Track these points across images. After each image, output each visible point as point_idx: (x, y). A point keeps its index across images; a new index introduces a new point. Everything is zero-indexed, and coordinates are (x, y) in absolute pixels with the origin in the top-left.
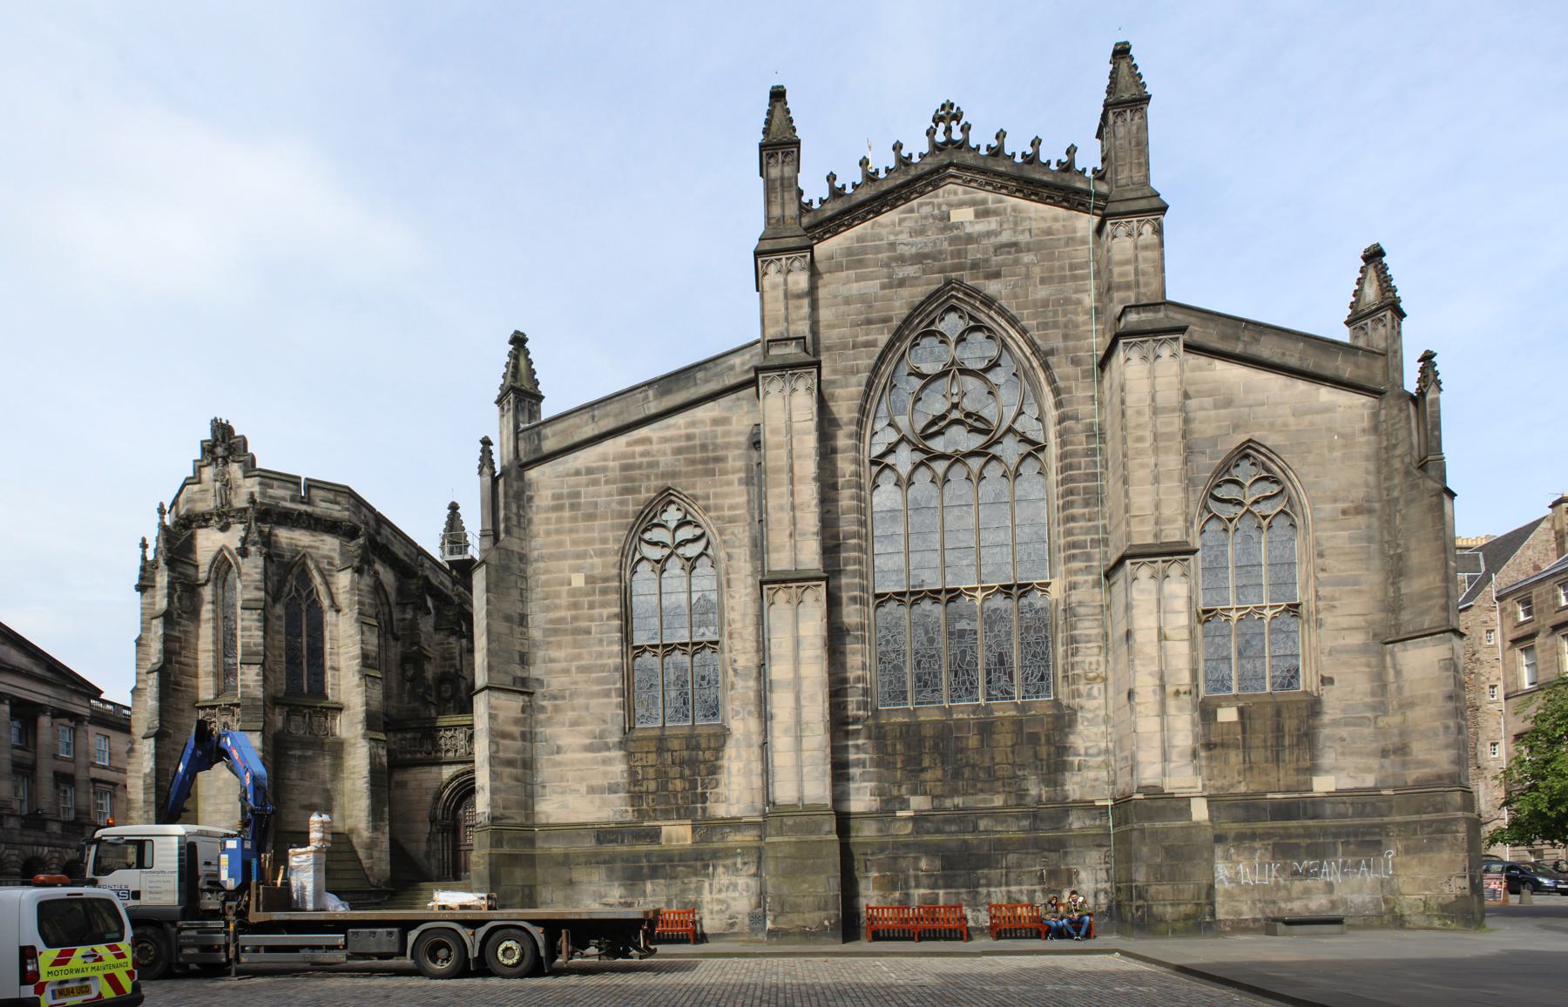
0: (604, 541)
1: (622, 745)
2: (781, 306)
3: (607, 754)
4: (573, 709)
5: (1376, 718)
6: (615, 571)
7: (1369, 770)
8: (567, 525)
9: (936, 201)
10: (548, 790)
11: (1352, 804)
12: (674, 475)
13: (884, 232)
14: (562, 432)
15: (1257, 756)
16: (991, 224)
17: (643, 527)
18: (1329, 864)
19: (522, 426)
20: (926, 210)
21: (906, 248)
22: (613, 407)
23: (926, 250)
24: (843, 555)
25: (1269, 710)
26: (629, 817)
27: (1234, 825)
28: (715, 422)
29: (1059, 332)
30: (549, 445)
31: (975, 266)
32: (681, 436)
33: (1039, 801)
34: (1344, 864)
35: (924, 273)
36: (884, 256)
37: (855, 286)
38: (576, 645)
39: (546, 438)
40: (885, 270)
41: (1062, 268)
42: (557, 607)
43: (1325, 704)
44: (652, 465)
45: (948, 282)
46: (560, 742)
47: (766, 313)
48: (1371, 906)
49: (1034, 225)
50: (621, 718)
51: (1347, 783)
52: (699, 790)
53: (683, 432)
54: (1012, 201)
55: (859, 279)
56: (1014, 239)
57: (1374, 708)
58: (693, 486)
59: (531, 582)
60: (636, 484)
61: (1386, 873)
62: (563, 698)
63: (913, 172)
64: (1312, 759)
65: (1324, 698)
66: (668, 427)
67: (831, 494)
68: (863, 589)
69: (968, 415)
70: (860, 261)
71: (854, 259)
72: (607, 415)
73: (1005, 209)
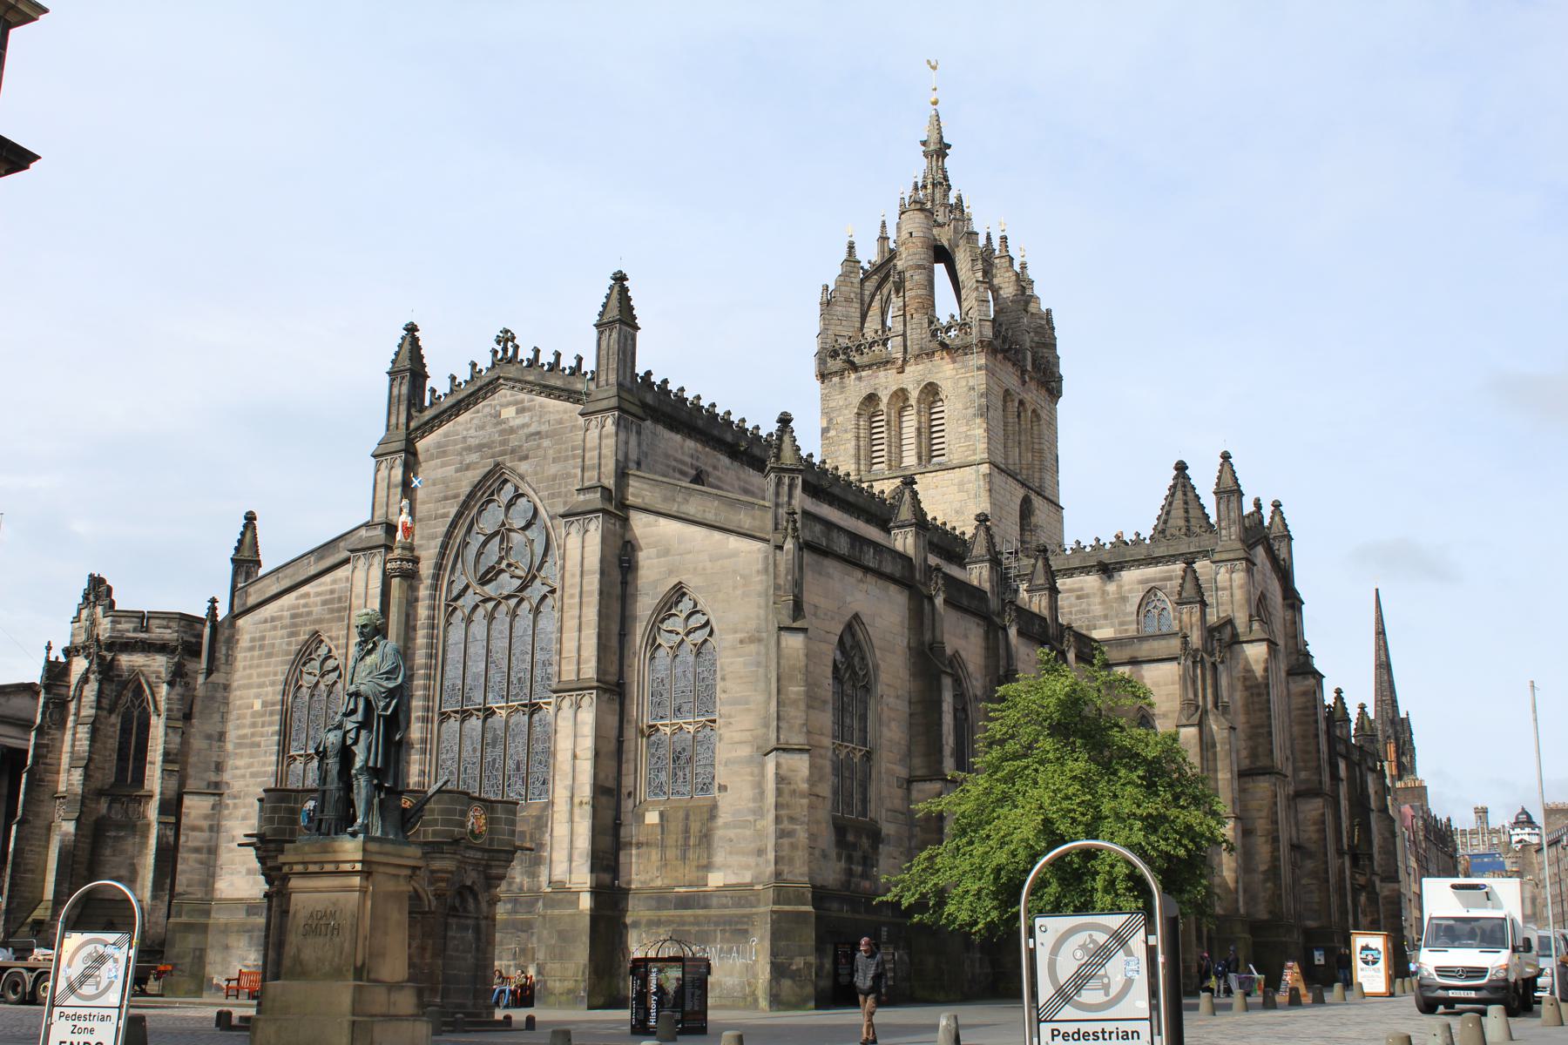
0: (275, 674)
2: (385, 493)
4: (245, 807)
5: (755, 821)
6: (280, 697)
7: (747, 867)
8: (255, 662)
9: (493, 403)
10: (224, 871)
11: (732, 898)
12: (320, 621)
13: (459, 428)
14: (260, 590)
15: (671, 853)
18: (710, 948)
19: (240, 585)
20: (487, 410)
21: (472, 440)
22: (289, 571)
23: (485, 441)
24: (415, 683)
25: (681, 814)
27: (647, 913)
30: (251, 601)
31: (513, 451)
32: (326, 591)
33: (521, 889)
34: (721, 949)
35: (482, 458)
37: (440, 470)
38: (252, 756)
41: (567, 450)
42: (243, 726)
43: (720, 808)
44: (309, 613)
45: (497, 465)
48: (738, 988)
49: (552, 417)
51: (732, 880)
53: (329, 588)
55: (444, 465)
56: (539, 429)
57: (754, 812)
58: (330, 630)
59: (231, 706)
61: (751, 959)
63: (479, 384)
64: (708, 858)
65: (719, 803)
66: (320, 585)
67: (411, 634)
70: (444, 452)
71: (441, 451)
72: (286, 577)
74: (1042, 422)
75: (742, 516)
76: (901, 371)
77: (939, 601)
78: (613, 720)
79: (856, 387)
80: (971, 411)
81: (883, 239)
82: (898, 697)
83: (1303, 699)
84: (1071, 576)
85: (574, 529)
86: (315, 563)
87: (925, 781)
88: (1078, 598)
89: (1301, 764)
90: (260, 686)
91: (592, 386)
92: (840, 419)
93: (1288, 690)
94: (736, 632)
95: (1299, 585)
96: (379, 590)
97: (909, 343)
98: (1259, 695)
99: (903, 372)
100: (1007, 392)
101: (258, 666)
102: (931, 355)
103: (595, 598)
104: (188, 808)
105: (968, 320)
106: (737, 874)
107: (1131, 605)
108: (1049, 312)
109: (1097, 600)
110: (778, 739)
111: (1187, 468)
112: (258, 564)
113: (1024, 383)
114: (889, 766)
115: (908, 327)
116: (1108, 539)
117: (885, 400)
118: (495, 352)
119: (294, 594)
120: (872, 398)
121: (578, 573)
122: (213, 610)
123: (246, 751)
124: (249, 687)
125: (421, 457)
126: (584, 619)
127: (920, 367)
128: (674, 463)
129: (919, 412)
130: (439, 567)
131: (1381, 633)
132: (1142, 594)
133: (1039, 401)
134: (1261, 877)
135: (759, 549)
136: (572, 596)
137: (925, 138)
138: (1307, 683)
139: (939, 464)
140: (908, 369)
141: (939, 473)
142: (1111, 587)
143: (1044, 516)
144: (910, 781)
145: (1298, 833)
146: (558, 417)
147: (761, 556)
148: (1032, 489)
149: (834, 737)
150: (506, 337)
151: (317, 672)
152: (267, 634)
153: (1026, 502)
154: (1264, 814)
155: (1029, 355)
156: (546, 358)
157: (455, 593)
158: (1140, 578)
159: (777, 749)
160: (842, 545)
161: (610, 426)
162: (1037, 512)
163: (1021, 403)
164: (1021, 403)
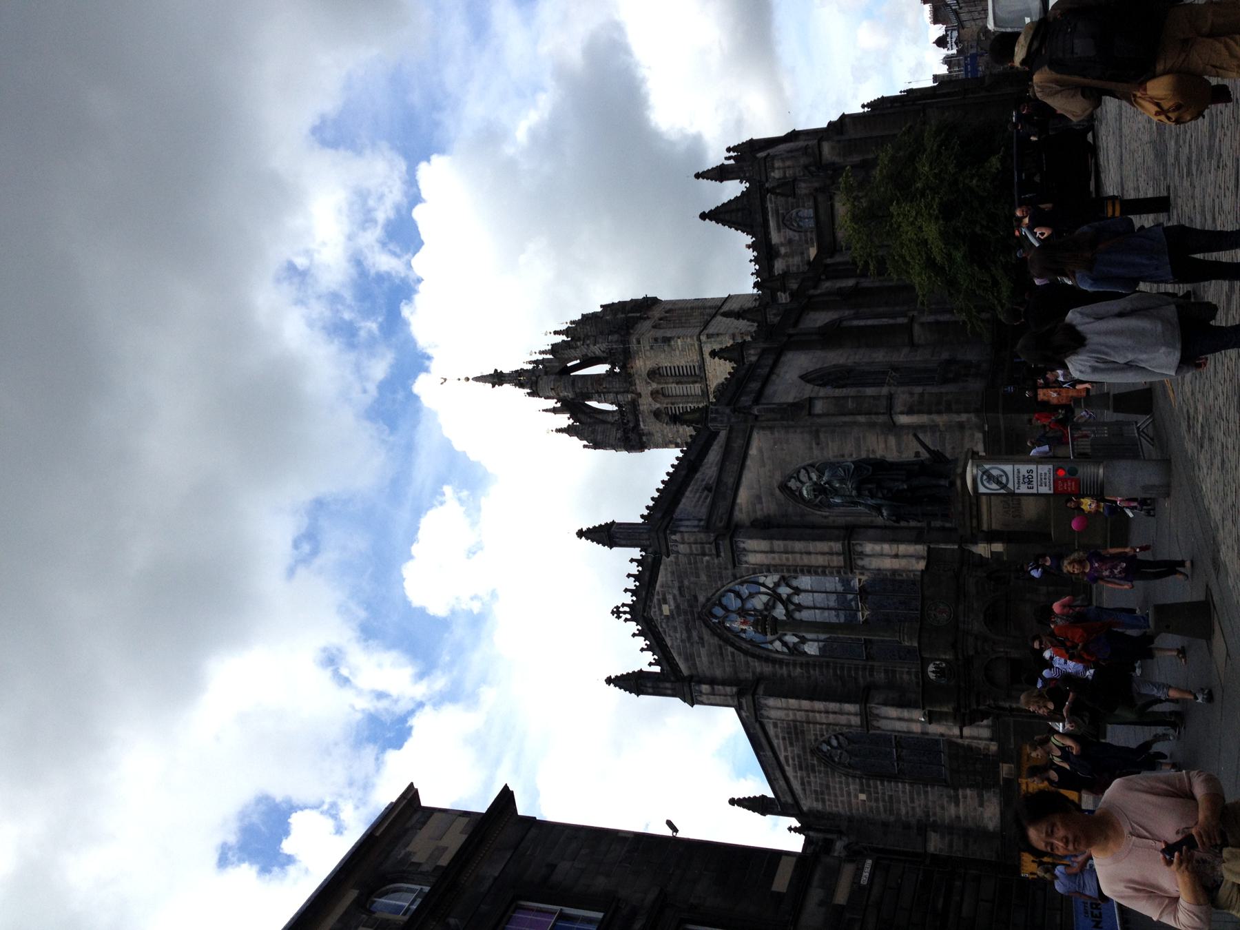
1: (956, 789)
2: (718, 697)
3: (960, 797)
8: (832, 798)
9: (659, 620)
12: (804, 748)
16: (670, 597)
17: (833, 764)
20: (664, 626)
23: (684, 626)
26: (998, 791)
28: (775, 725)
29: (724, 572)
30: (790, 800)
31: (691, 606)
32: (784, 743)
36: (688, 645)
37: (703, 658)
39: (786, 801)
40: (695, 645)
41: (691, 568)
42: (878, 808)
44: (799, 757)
45: (700, 618)
46: (954, 816)
47: (722, 703)
49: (670, 579)
50: (940, 788)
52: (982, 757)
53: (781, 741)
54: (658, 587)
55: (699, 656)
56: (677, 588)
58: (810, 740)
60: (810, 765)
62: (928, 812)
63: (646, 631)
68: (864, 669)
69: (766, 609)
71: (689, 658)
72: (774, 774)
73: (662, 591)
74: (673, 308)
75: (735, 445)
76: (639, 395)
77: (791, 331)
78: (871, 532)
79: (648, 425)
81: (555, 410)
82: (856, 354)
85: (745, 559)
86: (764, 751)
87: (912, 335)
90: (849, 794)
91: (650, 550)
92: (670, 435)
94: (811, 448)
96: (783, 700)
97: (622, 390)
99: (640, 394)
100: (654, 327)
101: (836, 795)
102: (630, 375)
103: (790, 544)
104: (936, 850)
105: (607, 351)
106: (977, 443)
107: (795, 236)
108: (602, 306)
109: (790, 260)
110: (883, 414)
111: (704, 212)
112: (763, 797)
113: (648, 318)
114: (901, 356)
115: (611, 390)
116: (751, 254)
117: (658, 405)
118: (626, 620)
119: (786, 768)
120: (657, 414)
121: (773, 555)
122: (796, 830)
123: (895, 806)
124: (850, 803)
125: (694, 672)
126: (803, 550)
127: (637, 382)
128: (700, 503)
129: (666, 383)
130: (767, 660)
132: (787, 230)
133: (660, 310)
135: (758, 433)
136: (787, 559)
137: (490, 385)
139: (700, 368)
140: (639, 390)
141: (706, 368)
142: (783, 250)
143: (735, 305)
144: (913, 345)
146: (669, 575)
147: (761, 432)
149: (883, 386)
150: (617, 612)
151: (839, 751)
152: (813, 788)
153: (727, 315)
156: (631, 583)
157: (785, 650)
158: (776, 231)
159: (891, 415)
160: (755, 386)
161: (677, 537)
162: (732, 308)
164: (661, 319)
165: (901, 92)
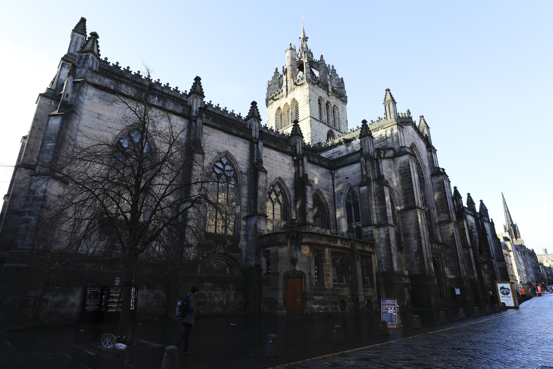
74: (339, 109)
80: (305, 102)
83: (438, 185)
84: (336, 147)
88: (339, 154)
89: (441, 210)
93: (432, 182)
95: (434, 144)
98: (407, 176)
108: (342, 79)
113: (329, 96)
131: (505, 203)
134: (414, 254)
138: (439, 178)
142: (350, 148)
145: (442, 237)
148: (334, 129)
154: (413, 226)
155: (330, 88)
163: (328, 102)
164: (328, 102)
165: (492, 219)
